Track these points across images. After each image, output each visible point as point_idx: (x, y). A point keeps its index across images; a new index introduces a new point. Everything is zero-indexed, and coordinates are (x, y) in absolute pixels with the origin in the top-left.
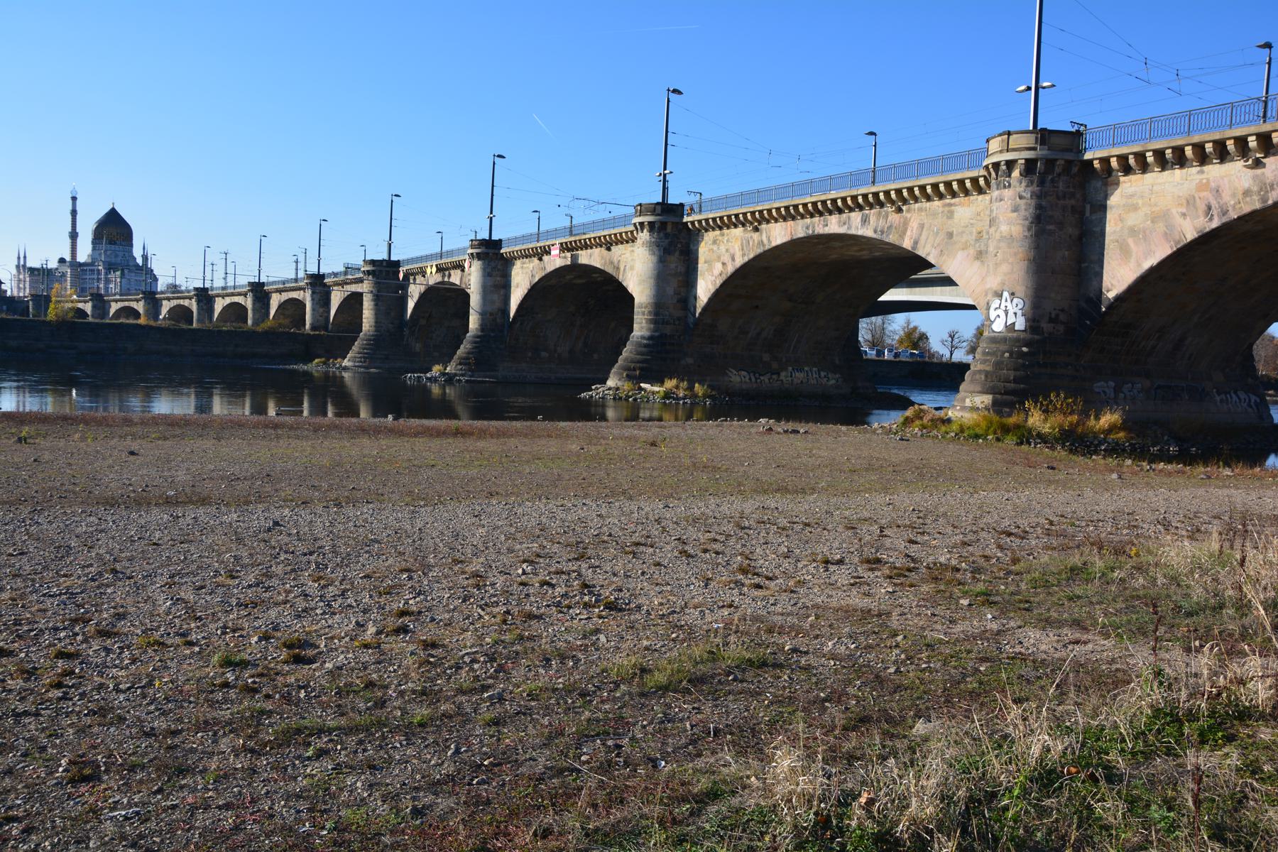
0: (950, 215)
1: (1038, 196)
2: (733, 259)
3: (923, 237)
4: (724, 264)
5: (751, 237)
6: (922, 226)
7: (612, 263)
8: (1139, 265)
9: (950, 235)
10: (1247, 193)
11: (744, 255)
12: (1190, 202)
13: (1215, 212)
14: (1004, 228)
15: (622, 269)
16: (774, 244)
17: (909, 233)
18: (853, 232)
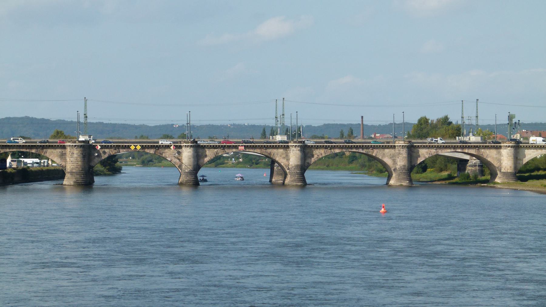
0: (384, 151)
1: (408, 151)
2: (321, 154)
3: (378, 153)
4: (318, 155)
5: (328, 150)
6: (377, 152)
7: (267, 152)
8: (420, 161)
9: (384, 154)
10: (435, 152)
11: (325, 154)
12: (427, 152)
13: (430, 154)
14: (404, 155)
15: (272, 154)
16: (336, 152)
17: (374, 153)
18: (360, 151)
